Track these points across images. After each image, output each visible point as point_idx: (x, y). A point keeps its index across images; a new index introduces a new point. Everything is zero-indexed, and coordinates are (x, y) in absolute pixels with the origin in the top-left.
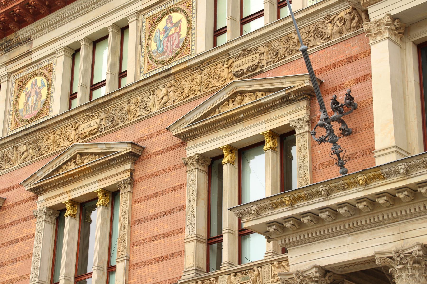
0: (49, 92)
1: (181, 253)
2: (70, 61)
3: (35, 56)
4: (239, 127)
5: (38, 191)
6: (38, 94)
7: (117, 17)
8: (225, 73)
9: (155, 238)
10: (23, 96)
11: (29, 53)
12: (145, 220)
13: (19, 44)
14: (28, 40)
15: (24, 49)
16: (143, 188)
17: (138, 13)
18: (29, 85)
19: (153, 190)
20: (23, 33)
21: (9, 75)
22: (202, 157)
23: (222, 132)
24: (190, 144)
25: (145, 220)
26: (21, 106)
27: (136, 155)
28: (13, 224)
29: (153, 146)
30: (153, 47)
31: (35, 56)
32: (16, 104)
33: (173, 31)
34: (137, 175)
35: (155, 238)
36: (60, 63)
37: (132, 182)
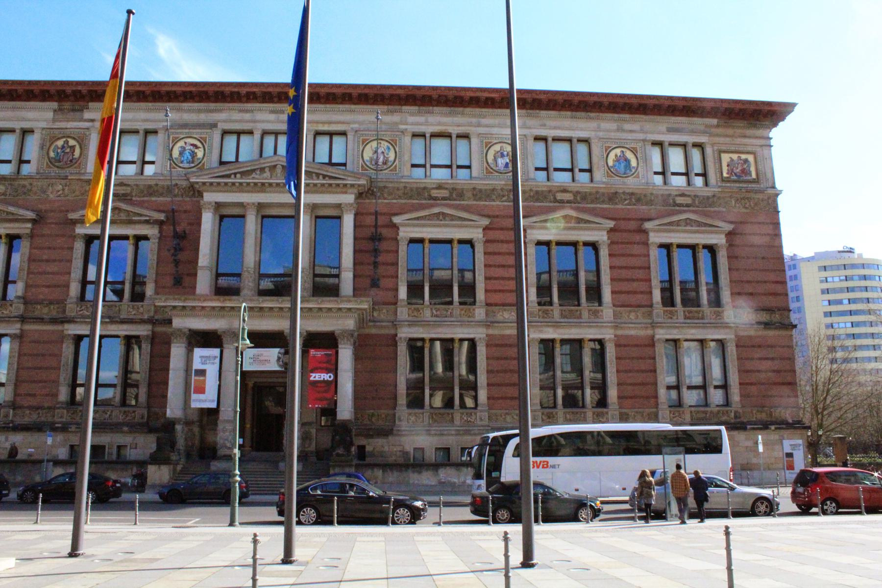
30: (52, 154)
33: (68, 150)
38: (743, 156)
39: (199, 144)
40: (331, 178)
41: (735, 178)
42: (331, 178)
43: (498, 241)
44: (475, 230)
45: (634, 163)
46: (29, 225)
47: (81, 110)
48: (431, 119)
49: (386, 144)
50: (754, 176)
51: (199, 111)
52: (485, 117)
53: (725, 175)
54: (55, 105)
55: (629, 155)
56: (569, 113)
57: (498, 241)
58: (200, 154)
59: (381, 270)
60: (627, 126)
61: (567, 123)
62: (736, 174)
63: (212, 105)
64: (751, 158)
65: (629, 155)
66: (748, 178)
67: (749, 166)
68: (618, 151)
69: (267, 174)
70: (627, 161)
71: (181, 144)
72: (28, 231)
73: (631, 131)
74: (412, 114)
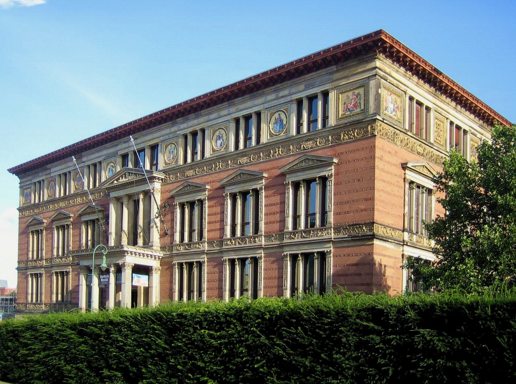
3: (52, 175)
14: (50, 169)
15: (48, 172)
20: (49, 166)
31: (52, 175)
45: (285, 123)
48: (190, 123)
49: (174, 146)
52: (210, 114)
53: (341, 113)
55: (283, 116)
56: (248, 96)
58: (114, 169)
60: (281, 94)
61: (249, 104)
63: (115, 143)
65: (283, 116)
68: (276, 115)
70: (281, 121)
71: (109, 167)
73: (282, 97)
74: (182, 123)
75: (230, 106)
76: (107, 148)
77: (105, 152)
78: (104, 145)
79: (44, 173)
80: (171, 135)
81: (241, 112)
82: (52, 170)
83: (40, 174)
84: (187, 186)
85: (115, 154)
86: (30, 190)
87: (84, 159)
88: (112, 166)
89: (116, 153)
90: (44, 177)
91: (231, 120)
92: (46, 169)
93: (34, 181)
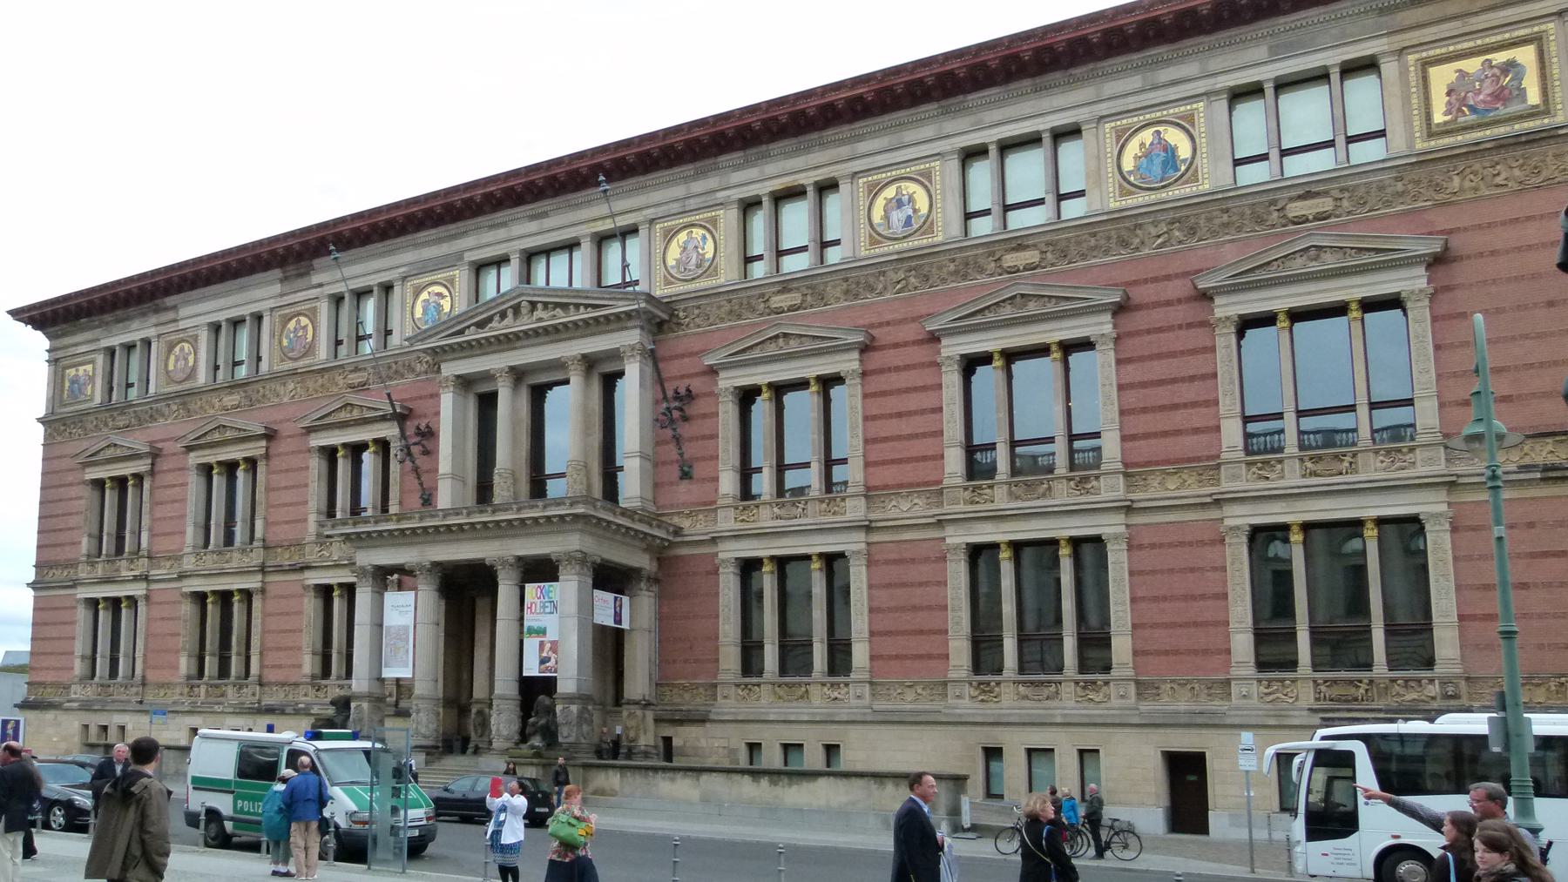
0: (195, 361)
1: (305, 520)
2: (213, 337)
3: (182, 324)
4: (350, 430)
5: (189, 449)
6: (186, 359)
7: (254, 308)
8: (341, 382)
9: (285, 505)
10: (172, 358)
11: (175, 321)
12: (278, 489)
13: (166, 309)
14: (175, 308)
15: (171, 315)
16: (276, 463)
17: (272, 309)
18: (177, 349)
19: (284, 466)
20: (170, 301)
21: (159, 336)
22: (322, 449)
23: (337, 432)
24: (313, 435)
25: (278, 489)
26: (171, 367)
27: (270, 436)
28: (169, 471)
29: (286, 429)
30: (285, 342)
31: (182, 324)
32: (166, 365)
34: (272, 451)
35: (285, 505)
36: (204, 336)
37: (267, 456)
38: (1500, 57)
39: (445, 292)
40: (595, 307)
41: (1470, 118)
42: (595, 307)
43: (889, 370)
44: (846, 356)
46: (263, 443)
47: (306, 274)
50: (1533, 97)
51: (439, 241)
54: (277, 273)
57: (889, 370)
59: (690, 450)
62: (1473, 109)
63: (452, 228)
64: (1526, 56)
66: (1515, 108)
67: (1519, 77)
69: (509, 319)
71: (424, 296)
72: (263, 451)
75: (946, 112)
76: (416, 246)
77: (409, 256)
78: (409, 237)
79: (153, 319)
80: (692, 201)
81: (996, 130)
82: (183, 312)
83: (135, 324)
84: (777, 337)
85: (453, 261)
86: (89, 367)
87: (316, 279)
88: (440, 295)
89: (459, 256)
90: (150, 332)
91: (952, 152)
92: (157, 311)
93: (105, 343)
